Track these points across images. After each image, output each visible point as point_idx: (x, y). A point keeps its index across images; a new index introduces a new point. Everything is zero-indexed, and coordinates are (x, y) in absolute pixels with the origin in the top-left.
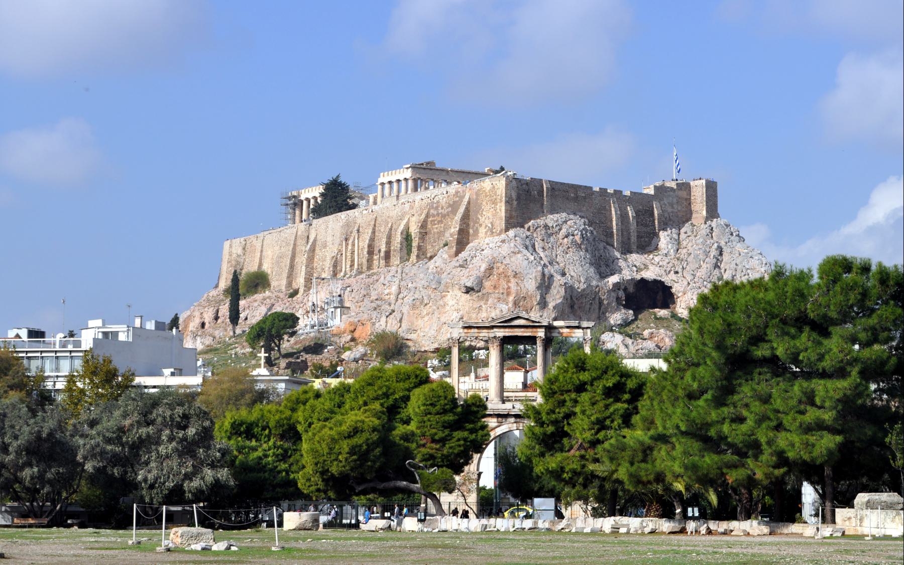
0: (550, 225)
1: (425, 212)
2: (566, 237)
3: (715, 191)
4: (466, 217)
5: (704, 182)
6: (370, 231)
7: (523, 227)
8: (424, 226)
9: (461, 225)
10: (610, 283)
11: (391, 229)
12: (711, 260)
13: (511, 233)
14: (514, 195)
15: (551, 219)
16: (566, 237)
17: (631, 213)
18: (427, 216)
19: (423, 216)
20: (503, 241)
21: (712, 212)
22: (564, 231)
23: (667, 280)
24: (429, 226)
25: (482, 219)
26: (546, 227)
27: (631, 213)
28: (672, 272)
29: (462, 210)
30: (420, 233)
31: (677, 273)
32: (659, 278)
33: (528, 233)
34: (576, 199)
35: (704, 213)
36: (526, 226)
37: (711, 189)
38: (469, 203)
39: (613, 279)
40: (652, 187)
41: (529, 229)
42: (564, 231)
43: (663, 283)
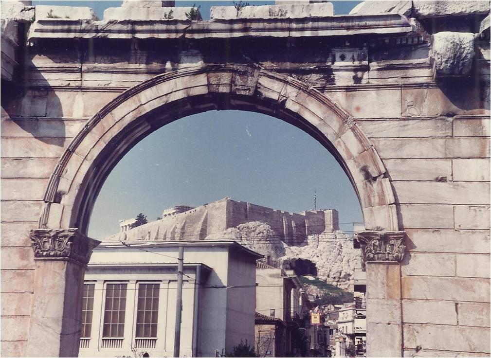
0: (250, 227)
1: (184, 221)
2: (259, 233)
3: (337, 216)
4: (205, 221)
5: (331, 211)
6: (156, 233)
7: (235, 227)
8: (183, 228)
9: (202, 226)
10: (282, 260)
11: (166, 232)
12: (336, 251)
13: (230, 230)
14: (231, 210)
15: (251, 224)
16: (259, 233)
17: (293, 224)
18: (185, 224)
19: (183, 224)
20: (225, 234)
21: (336, 227)
22: (257, 231)
23: (314, 260)
24: (186, 228)
25: (214, 223)
26: (248, 228)
27: (293, 224)
28: (315, 256)
29: (203, 219)
30: (181, 232)
31: (318, 257)
32: (309, 259)
33: (238, 231)
34: (265, 214)
35: (332, 226)
36: (238, 227)
37: (335, 214)
38: (207, 214)
39: (284, 258)
40: (304, 212)
41: (239, 229)
42: (257, 231)
43: (311, 262)
